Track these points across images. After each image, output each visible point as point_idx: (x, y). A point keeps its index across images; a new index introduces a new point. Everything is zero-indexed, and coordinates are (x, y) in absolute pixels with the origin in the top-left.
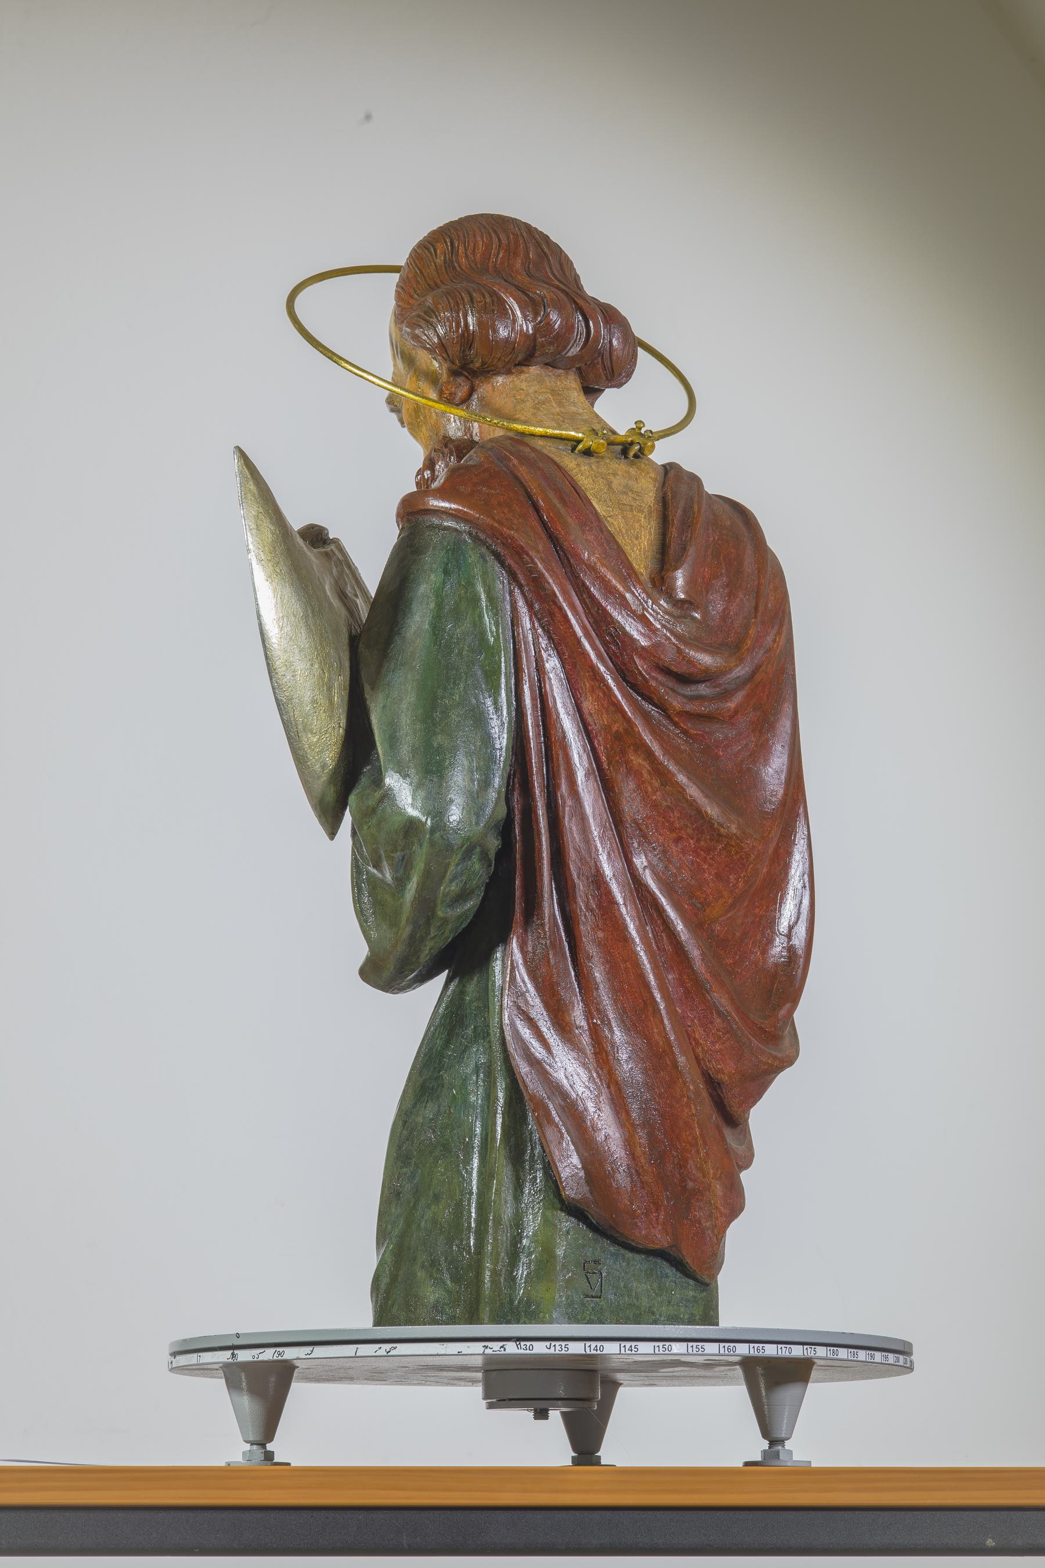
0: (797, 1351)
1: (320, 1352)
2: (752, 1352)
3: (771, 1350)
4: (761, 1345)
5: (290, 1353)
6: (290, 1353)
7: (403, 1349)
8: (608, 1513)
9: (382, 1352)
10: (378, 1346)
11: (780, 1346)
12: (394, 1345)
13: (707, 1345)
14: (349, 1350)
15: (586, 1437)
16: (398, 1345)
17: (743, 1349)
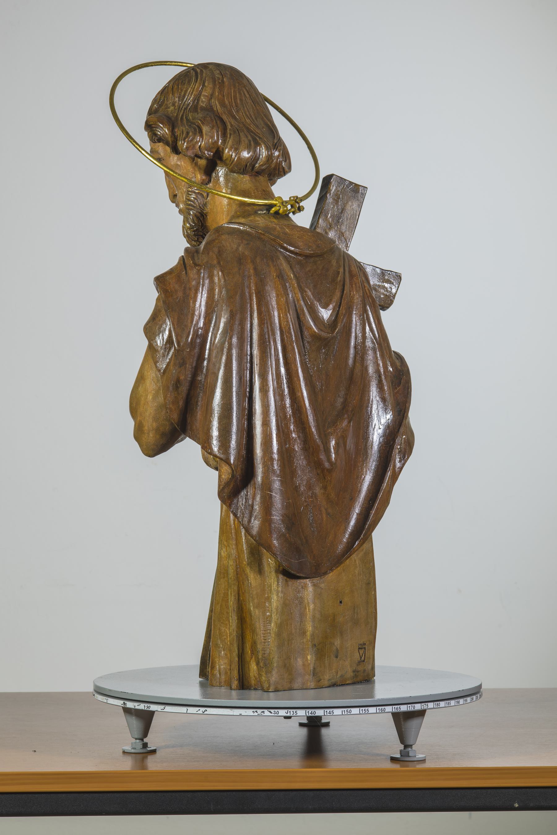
0: (418, 707)
1: (168, 709)
2: (394, 710)
3: (404, 708)
4: (398, 706)
5: (153, 708)
6: (153, 708)
7: (210, 711)
8: (318, 792)
9: (200, 712)
10: (197, 709)
11: (408, 706)
12: (206, 709)
14: (183, 710)
15: (314, 726)
16: (208, 709)
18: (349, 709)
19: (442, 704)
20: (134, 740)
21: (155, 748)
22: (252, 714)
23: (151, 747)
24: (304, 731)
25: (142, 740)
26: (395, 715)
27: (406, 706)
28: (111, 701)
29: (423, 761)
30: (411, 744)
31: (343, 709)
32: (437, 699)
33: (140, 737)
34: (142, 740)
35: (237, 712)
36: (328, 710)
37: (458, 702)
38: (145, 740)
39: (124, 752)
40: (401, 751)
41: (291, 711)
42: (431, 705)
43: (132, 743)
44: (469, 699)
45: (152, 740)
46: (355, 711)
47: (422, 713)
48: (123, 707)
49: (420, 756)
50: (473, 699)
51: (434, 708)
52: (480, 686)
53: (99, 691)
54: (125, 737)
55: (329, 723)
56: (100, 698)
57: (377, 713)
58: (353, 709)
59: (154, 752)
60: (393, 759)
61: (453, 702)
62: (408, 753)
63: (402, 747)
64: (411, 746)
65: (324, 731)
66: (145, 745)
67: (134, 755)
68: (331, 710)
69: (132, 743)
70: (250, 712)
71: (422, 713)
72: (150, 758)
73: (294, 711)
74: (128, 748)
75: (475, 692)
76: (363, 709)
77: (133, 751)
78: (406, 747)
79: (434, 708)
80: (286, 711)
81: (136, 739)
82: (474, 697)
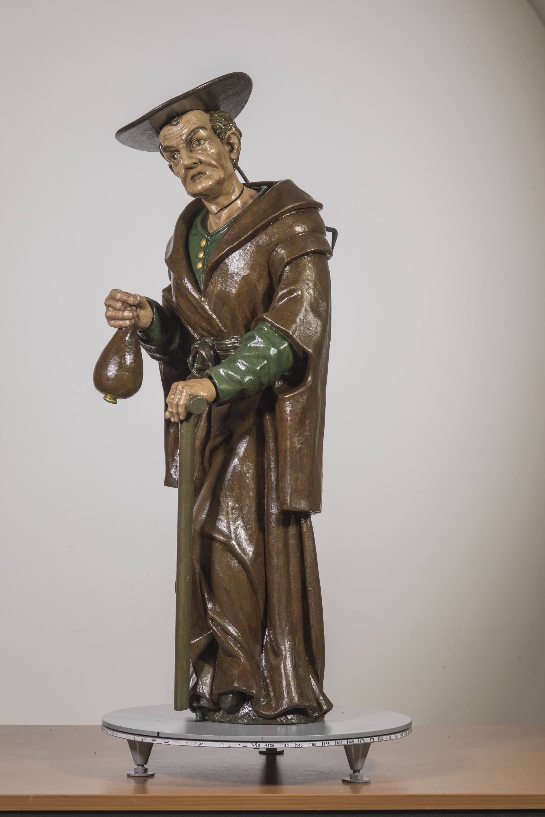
0: (367, 740)
13: (330, 742)
14: (183, 743)
17: (345, 742)
18: (314, 742)
19: (385, 738)
20: (136, 767)
21: (153, 773)
22: (239, 746)
23: (149, 772)
24: (263, 758)
25: (143, 766)
26: (347, 747)
27: (357, 740)
28: (121, 735)
29: (368, 783)
30: (359, 769)
31: (310, 743)
32: (380, 735)
33: (142, 764)
34: (143, 766)
35: (226, 745)
36: (298, 743)
37: (396, 736)
38: (146, 766)
39: (129, 776)
40: (350, 776)
41: (270, 744)
42: (376, 739)
43: (135, 769)
44: (404, 734)
45: (151, 766)
46: (319, 744)
47: (367, 746)
48: (129, 741)
49: (365, 779)
50: (406, 733)
51: (378, 741)
52: (410, 724)
53: (108, 727)
54: (128, 763)
55: (283, 751)
56: (110, 732)
57: (335, 745)
58: (317, 743)
59: (152, 776)
60: (345, 782)
61: (392, 737)
62: (357, 776)
63: (351, 772)
64: (358, 771)
65: (279, 758)
66: (146, 770)
67: (137, 778)
68: (301, 743)
69: (135, 769)
70: (237, 745)
71: (367, 746)
72: (149, 781)
73: (272, 744)
74: (132, 772)
75: (407, 729)
76: (325, 742)
77: (137, 775)
78: (355, 771)
79: (378, 741)
80: (266, 744)
81: (138, 765)
82: (408, 732)
